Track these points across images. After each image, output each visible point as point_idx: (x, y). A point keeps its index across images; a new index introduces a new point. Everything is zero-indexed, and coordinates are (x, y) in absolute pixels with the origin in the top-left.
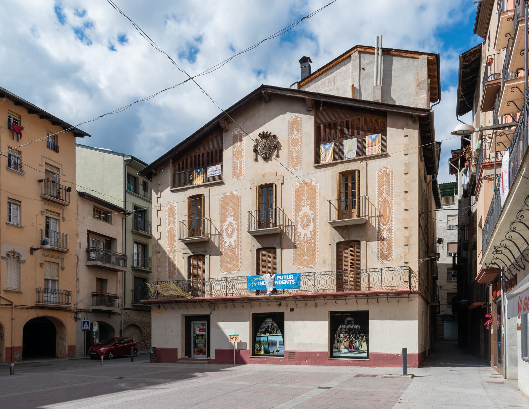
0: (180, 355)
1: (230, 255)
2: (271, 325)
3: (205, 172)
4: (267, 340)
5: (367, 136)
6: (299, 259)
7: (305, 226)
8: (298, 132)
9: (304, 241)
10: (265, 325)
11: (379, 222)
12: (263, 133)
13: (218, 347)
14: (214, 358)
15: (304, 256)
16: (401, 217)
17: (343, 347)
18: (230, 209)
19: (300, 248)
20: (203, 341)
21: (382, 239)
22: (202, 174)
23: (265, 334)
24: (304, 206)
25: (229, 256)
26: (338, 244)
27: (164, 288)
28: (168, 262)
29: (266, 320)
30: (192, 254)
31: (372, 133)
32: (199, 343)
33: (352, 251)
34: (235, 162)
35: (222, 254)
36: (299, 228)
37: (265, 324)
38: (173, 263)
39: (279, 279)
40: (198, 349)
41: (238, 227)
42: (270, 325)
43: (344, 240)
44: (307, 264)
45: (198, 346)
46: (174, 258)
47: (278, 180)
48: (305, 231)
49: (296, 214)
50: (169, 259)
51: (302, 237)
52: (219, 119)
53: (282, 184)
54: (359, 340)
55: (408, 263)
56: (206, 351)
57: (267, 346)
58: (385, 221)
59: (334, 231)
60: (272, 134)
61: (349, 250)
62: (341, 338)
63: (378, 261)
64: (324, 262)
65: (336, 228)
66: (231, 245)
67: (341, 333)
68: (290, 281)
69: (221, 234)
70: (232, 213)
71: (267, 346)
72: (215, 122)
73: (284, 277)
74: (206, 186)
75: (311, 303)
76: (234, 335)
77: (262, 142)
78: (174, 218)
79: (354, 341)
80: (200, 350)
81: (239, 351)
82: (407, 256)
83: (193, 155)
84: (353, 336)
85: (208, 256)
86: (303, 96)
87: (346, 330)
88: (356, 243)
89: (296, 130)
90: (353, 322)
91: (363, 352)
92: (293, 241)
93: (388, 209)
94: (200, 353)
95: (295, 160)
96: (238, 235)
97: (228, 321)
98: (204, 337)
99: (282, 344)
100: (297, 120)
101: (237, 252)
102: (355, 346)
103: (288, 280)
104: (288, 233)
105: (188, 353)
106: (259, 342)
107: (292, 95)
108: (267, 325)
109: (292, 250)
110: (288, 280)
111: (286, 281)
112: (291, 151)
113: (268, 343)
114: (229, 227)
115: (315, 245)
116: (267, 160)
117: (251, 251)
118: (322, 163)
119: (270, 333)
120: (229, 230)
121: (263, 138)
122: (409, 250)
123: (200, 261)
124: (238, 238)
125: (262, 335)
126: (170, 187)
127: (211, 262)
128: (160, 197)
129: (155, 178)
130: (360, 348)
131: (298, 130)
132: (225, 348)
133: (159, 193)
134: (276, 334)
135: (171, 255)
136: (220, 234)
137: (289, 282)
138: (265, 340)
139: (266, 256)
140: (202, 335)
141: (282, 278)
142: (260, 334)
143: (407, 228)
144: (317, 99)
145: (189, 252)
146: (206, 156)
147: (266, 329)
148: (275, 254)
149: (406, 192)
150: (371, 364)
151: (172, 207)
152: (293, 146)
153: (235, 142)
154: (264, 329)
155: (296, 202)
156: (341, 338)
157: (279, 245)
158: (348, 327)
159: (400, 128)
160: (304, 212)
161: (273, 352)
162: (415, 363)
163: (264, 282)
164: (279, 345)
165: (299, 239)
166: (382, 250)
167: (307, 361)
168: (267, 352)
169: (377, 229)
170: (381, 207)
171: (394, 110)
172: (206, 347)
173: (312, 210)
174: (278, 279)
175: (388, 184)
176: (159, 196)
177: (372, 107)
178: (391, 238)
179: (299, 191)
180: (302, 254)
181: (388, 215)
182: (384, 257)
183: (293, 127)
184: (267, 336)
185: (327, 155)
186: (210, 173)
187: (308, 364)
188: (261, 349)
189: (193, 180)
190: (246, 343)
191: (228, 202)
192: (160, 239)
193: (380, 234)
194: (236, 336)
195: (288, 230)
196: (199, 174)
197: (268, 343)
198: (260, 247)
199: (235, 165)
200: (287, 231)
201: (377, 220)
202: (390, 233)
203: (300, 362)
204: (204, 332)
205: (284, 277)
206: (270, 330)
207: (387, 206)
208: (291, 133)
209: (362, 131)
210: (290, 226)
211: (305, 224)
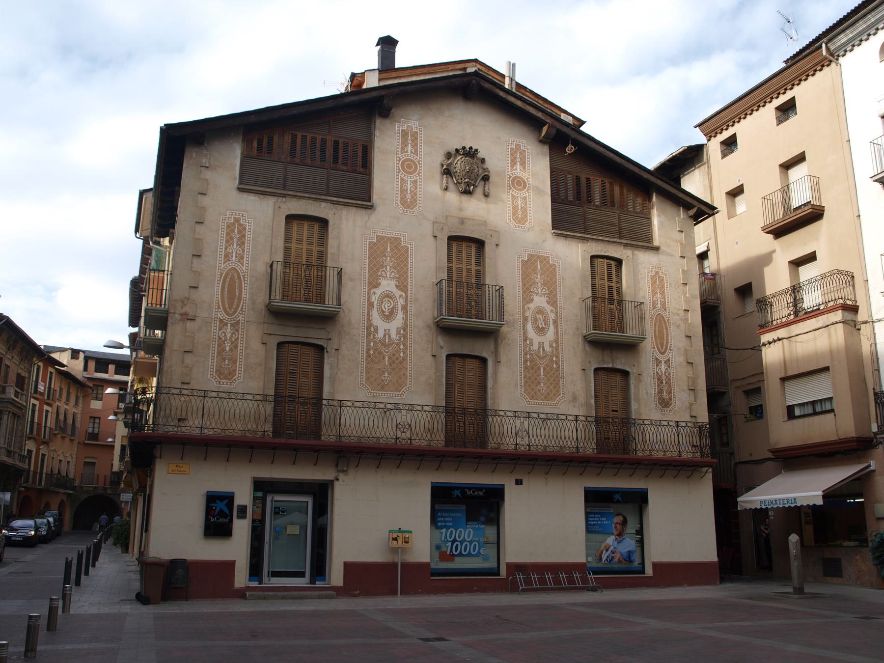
1: (387, 358)
6: (530, 386)
7: (541, 331)
8: (524, 168)
12: (471, 148)
15: (539, 383)
16: (683, 346)
18: (388, 263)
24: (537, 294)
25: (384, 358)
34: (402, 179)
44: (545, 398)
46: (238, 338)
58: (662, 348)
63: (656, 409)
64: (575, 399)
66: (390, 336)
77: (460, 164)
78: (243, 251)
89: (521, 164)
93: (665, 330)
95: (520, 213)
96: (406, 319)
101: (404, 353)
112: (512, 195)
114: (386, 299)
115: (559, 367)
120: (386, 306)
124: (407, 326)
151: (240, 225)
155: (524, 285)
160: (538, 305)
165: (530, 349)
166: (660, 391)
175: (663, 293)
178: (671, 375)
181: (665, 339)
183: (515, 158)
199: (401, 185)
202: (669, 367)
207: (663, 325)
211: (540, 326)
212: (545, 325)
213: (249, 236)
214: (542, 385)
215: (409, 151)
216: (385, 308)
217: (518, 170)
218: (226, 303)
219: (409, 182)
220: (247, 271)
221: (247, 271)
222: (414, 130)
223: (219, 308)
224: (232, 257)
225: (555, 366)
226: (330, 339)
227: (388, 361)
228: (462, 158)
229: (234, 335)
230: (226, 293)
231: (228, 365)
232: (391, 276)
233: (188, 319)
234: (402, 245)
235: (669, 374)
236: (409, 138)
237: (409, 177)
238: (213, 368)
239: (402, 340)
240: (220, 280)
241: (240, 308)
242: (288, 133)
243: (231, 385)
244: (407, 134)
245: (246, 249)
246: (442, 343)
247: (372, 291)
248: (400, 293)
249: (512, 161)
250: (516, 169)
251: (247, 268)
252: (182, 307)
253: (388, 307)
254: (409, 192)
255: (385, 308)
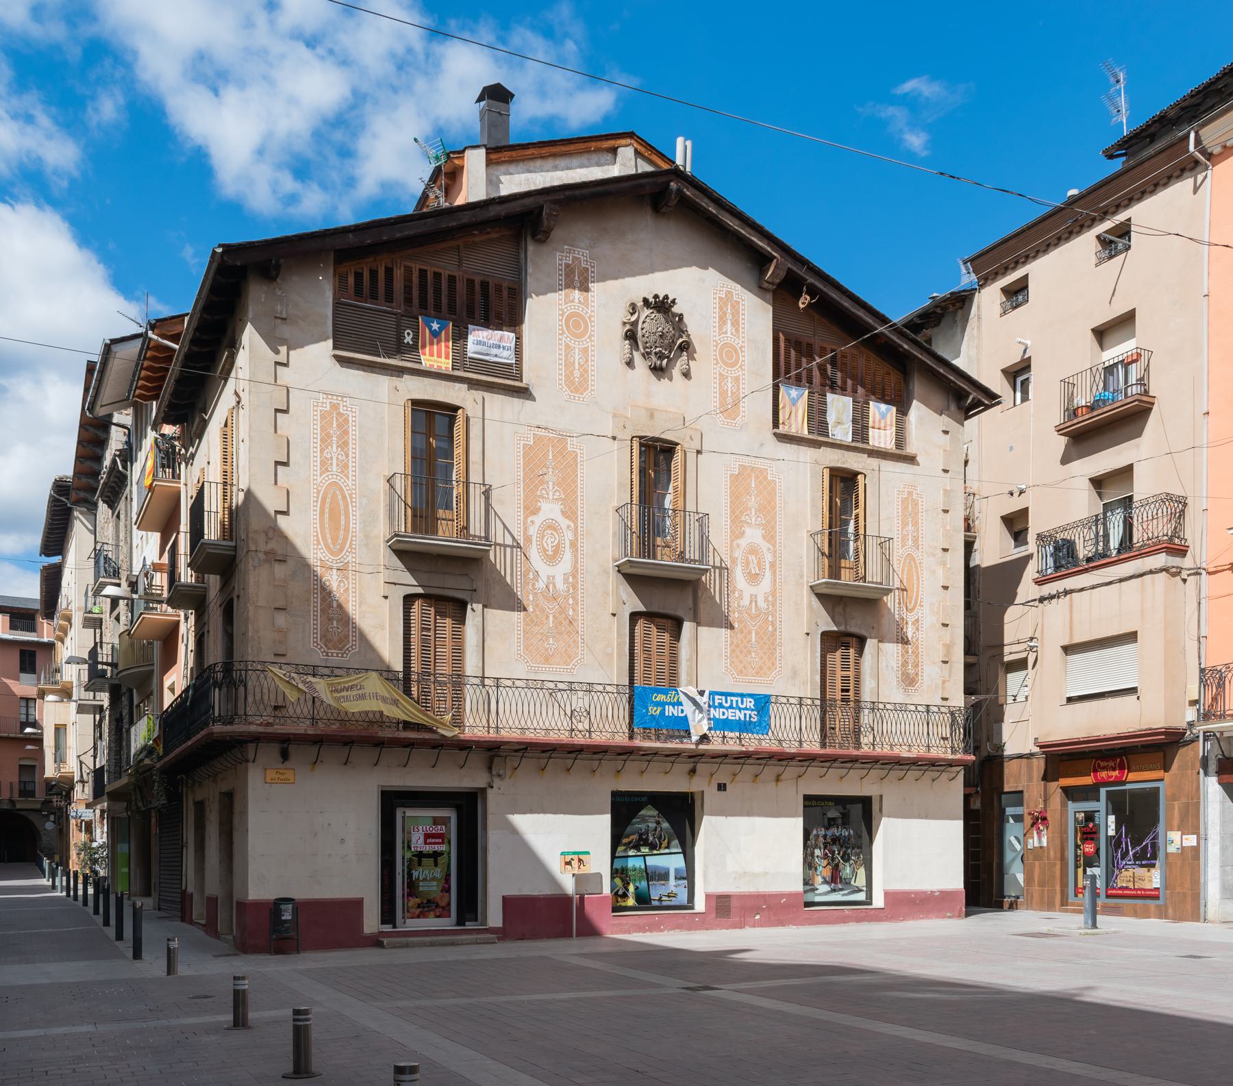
0: (371, 922)
2: (654, 825)
3: (460, 336)
4: (643, 867)
5: (871, 403)
7: (754, 578)
8: (737, 330)
9: (749, 615)
10: (637, 825)
11: (900, 603)
12: (666, 297)
13: (513, 891)
14: (501, 925)
15: (749, 652)
17: (819, 879)
19: (742, 632)
20: (438, 873)
21: (904, 641)
22: (447, 340)
23: (639, 851)
24: (749, 524)
25: (547, 618)
26: (825, 635)
27: (341, 690)
28: (323, 600)
29: (643, 812)
30: (420, 590)
31: (879, 398)
32: (425, 880)
33: (845, 658)
34: (567, 346)
35: (525, 609)
36: (739, 579)
37: (638, 823)
38: (340, 606)
39: (721, 706)
40: (418, 900)
41: (576, 535)
42: (652, 825)
43: (835, 629)
44: (757, 673)
45: (421, 889)
46: (347, 589)
47: (688, 437)
48: (753, 590)
49: (732, 541)
50: (326, 594)
51: (746, 602)
52: (540, 199)
53: (699, 452)
54: (851, 862)
55: (947, 699)
56: (449, 904)
57: (644, 883)
58: (910, 603)
59: (816, 603)
60: (675, 309)
61: (838, 653)
62: (817, 860)
64: (795, 674)
65: (822, 597)
66: (554, 586)
67: (816, 846)
68: (748, 712)
69: (520, 548)
70: (557, 494)
71: (643, 882)
72: (527, 201)
73: (732, 701)
74: (474, 384)
75: (770, 771)
76: (574, 853)
77: (650, 322)
78: (347, 456)
79: (841, 866)
80: (429, 901)
81: (582, 899)
82: (947, 684)
83: (412, 265)
84: (839, 854)
85: (481, 606)
86: (769, 249)
87: (825, 839)
88: (854, 639)
90: (840, 821)
91: (860, 891)
92: (725, 608)
94: (429, 911)
96: (576, 561)
97: (544, 811)
98: (441, 860)
99: (688, 875)
100: (724, 296)
101: (574, 610)
102: (843, 877)
103: (743, 709)
104: (712, 586)
105: (388, 915)
106: (622, 873)
107: (743, 232)
108: (643, 826)
109: (724, 632)
110: (743, 709)
111: (737, 711)
113: (647, 874)
114: (549, 532)
115: (775, 630)
116: (660, 373)
117: (614, 615)
118: (782, 429)
119: (653, 847)
120: (549, 542)
121: (659, 312)
122: (950, 672)
123: (443, 615)
124: (577, 571)
125: (631, 853)
126: (330, 342)
127: (488, 629)
128: (286, 365)
129: (265, 288)
130: (852, 882)
131: (736, 324)
132: (536, 893)
133: (283, 349)
134: (667, 851)
135: (333, 581)
136: (519, 546)
137: (745, 714)
138: (637, 866)
139: (657, 637)
140: (435, 855)
141: (726, 702)
142: (625, 850)
143: (947, 625)
144: (800, 273)
145: (409, 583)
146: (461, 287)
147: (641, 835)
148: (677, 635)
149: (945, 550)
150: (886, 917)
151: (340, 414)
152: (726, 364)
153: (567, 287)
154: (635, 837)
155: (733, 512)
156: (817, 860)
157: (692, 612)
158: (829, 833)
159: (935, 411)
160: (750, 541)
161: (660, 900)
162: (961, 908)
163: (680, 707)
164: (676, 878)
166: (905, 664)
167: (758, 917)
168: (643, 901)
169: (897, 616)
170: (903, 570)
171: (942, 371)
172: (448, 890)
173: (769, 541)
174: (716, 704)
175: (915, 524)
176: (282, 358)
177: (906, 346)
179: (737, 483)
180: (745, 647)
182: (909, 680)
183: (725, 314)
184: (644, 856)
185: (793, 414)
186: (479, 348)
187: (761, 924)
188: (628, 891)
189: (414, 348)
190: (599, 876)
191: (546, 455)
192: (286, 513)
193: (902, 629)
194: (581, 857)
195: (712, 578)
196: (435, 334)
197: (647, 874)
198: (641, 608)
200: (710, 579)
201: (897, 597)
202: (917, 629)
203: (742, 919)
204: (443, 843)
205: (732, 701)
206: (651, 838)
208: (721, 327)
209: (862, 386)
210: (717, 567)
211: (753, 572)
212: (759, 570)
213: (354, 433)
214: (753, 655)
215: (577, 301)
216: (548, 545)
217: (729, 335)
218: (328, 536)
219: (577, 350)
220: (354, 487)
221: (354, 487)
222: (583, 265)
223: (318, 543)
224: (331, 464)
225: (770, 628)
226: (475, 590)
227: (553, 622)
228: (652, 313)
229: (342, 584)
230: (326, 521)
231: (338, 628)
232: (555, 497)
233: (276, 560)
234: (569, 449)
235: (917, 640)
236: (577, 278)
237: (577, 343)
238: (317, 633)
239: (571, 591)
240: (317, 501)
241: (348, 544)
242: (398, 265)
243: (342, 657)
244: (572, 271)
245: (350, 453)
246: (624, 597)
247: (529, 520)
248: (568, 522)
249: (721, 318)
250: (726, 333)
251: (354, 483)
252: (267, 543)
253: (552, 542)
254: (577, 368)
255: (548, 545)
